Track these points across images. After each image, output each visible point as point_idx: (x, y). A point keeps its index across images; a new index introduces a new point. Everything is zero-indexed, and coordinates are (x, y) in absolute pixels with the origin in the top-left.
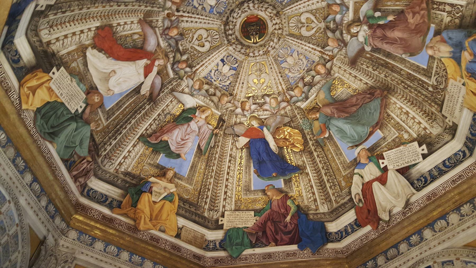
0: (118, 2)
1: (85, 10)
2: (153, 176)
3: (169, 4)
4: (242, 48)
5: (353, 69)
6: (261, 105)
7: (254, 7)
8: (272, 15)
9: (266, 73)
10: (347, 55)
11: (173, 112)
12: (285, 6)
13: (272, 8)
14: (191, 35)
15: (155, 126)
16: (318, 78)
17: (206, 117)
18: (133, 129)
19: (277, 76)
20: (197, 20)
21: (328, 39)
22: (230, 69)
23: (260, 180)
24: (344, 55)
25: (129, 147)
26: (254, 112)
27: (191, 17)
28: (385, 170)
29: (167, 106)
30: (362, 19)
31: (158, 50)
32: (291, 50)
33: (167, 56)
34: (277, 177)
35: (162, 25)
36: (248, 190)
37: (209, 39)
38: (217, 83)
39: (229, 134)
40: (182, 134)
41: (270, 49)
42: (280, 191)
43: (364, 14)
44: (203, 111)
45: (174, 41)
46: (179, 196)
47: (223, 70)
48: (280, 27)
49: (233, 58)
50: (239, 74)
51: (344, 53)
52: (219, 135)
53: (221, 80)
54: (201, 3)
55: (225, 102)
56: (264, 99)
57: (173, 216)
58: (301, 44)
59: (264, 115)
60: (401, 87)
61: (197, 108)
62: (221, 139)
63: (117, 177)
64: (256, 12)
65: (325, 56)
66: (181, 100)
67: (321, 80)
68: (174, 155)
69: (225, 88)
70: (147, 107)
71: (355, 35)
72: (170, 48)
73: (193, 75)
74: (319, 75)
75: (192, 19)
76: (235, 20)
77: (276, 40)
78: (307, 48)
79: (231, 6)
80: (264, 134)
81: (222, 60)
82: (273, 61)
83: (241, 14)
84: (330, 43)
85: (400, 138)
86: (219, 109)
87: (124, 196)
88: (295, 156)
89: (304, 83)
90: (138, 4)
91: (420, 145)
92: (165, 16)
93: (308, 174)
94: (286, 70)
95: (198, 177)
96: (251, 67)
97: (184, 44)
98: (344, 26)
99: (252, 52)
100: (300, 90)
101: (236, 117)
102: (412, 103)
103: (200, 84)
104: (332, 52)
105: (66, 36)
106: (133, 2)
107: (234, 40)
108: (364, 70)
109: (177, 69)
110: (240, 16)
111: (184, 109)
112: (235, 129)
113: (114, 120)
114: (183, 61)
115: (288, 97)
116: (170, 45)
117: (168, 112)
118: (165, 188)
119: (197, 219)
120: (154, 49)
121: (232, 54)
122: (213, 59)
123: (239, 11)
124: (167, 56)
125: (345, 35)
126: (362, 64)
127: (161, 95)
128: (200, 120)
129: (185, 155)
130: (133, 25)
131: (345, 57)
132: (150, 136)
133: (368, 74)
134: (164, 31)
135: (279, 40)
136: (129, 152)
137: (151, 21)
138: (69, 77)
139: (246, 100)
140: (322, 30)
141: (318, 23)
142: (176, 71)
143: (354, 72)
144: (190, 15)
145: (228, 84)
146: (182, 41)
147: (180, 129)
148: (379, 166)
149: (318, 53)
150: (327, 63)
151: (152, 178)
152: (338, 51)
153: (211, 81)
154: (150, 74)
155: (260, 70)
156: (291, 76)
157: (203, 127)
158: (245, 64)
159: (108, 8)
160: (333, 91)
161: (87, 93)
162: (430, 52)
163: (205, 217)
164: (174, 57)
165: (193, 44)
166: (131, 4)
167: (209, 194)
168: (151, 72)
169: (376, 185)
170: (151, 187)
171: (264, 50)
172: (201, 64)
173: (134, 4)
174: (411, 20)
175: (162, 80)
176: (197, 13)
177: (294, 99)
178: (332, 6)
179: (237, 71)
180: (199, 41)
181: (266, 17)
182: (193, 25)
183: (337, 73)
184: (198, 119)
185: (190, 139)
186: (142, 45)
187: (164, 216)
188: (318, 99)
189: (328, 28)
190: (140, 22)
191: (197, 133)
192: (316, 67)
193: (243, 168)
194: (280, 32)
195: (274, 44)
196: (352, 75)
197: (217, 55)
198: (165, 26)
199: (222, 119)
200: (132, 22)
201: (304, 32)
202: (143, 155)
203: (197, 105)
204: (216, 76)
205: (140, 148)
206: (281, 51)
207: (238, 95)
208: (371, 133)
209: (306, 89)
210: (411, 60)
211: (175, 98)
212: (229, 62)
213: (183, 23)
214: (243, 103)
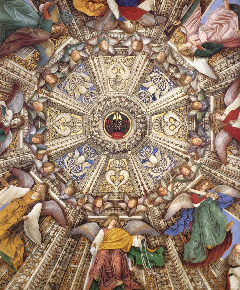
3: (194, 169)
4: (132, 107)
5: (16, 80)
6: (119, 44)
7: (115, 145)
9: (110, 79)
10: (24, 95)
12: (85, 143)
13: (98, 142)
16: (54, 70)
17: (186, 43)
19: (98, 74)
20: (171, 145)
21: (44, 110)
22: (148, 88)
24: (26, 94)
27: (176, 149)
29: (227, 67)
30: (10, 132)
32: (81, 99)
33: (211, 121)
35: (206, 152)
37: (163, 124)
38: (165, 77)
39: (163, 15)
40: (219, 32)
41: (103, 103)
43: (9, 136)
44: (187, 50)
45: (199, 133)
47: (155, 90)
48: (91, 124)
49: (143, 99)
50: (139, 82)
51: (26, 96)
52: (175, 17)
53: (160, 79)
54: (164, 160)
55: (160, 54)
56: (115, 50)
58: (71, 105)
61: (193, 56)
62: (173, 12)
64: (113, 141)
65: (47, 92)
67: (50, 67)
68: (237, 10)
69: (157, 70)
72: (205, 127)
73: (189, 91)
74: (53, 73)
75: (175, 147)
76: (135, 136)
77: (97, 111)
78: (65, 101)
81: (154, 99)
82: (102, 91)
83: (128, 141)
84: (41, 105)
86: (168, 48)
89: (69, 65)
90: (222, 180)
94: (88, 80)
96: (126, 87)
97: (190, 126)
98: (28, 124)
99: (122, 101)
100: (74, 58)
101: (150, 34)
103: (184, 81)
104: (39, 96)
106: (227, 184)
108: (4, 79)
109: (205, 103)
110: (129, 139)
111: (209, 59)
112: (153, 21)
114: (195, 109)
116: (204, 130)
117: (228, 61)
120: (222, 133)
121: (143, 103)
122: (164, 103)
123: (129, 144)
124: (211, 121)
125: (27, 115)
127: (230, 81)
129: (224, 6)
130: (234, 163)
131: (25, 92)
134: (205, 146)
135: (93, 111)
137: (215, 159)
141: (53, 125)
142: (206, 102)
144: (177, 152)
145: (153, 73)
146: (191, 130)
147: (220, 38)
149: (54, 95)
150: (44, 85)
153: (171, 80)
154: (235, 109)
155: (116, 82)
156: (83, 73)
157: (192, 33)
158: (131, 90)
160: (36, 57)
164: (204, 116)
165: (180, 123)
166: (229, 184)
168: (233, 112)
171: (110, 102)
172: (177, 101)
173: (226, 182)
175: (224, 98)
176: (169, 152)
178: (39, 142)
179: (141, 86)
180: (175, 125)
182: (176, 142)
184: (196, 43)
185: (210, 22)
186: (232, 141)
188: (53, 47)
189: (44, 121)
190: (227, 163)
191: (202, 27)
192: (55, 81)
194: (92, 119)
195: (98, 107)
196: (17, 74)
197: (159, 105)
198: (203, 149)
199: (167, 35)
200: (234, 166)
203: (193, 59)
204: (165, 84)
206: (92, 100)
207: (144, 59)
211: (215, 72)
212: (148, 96)
213: (185, 146)
214: (140, 49)
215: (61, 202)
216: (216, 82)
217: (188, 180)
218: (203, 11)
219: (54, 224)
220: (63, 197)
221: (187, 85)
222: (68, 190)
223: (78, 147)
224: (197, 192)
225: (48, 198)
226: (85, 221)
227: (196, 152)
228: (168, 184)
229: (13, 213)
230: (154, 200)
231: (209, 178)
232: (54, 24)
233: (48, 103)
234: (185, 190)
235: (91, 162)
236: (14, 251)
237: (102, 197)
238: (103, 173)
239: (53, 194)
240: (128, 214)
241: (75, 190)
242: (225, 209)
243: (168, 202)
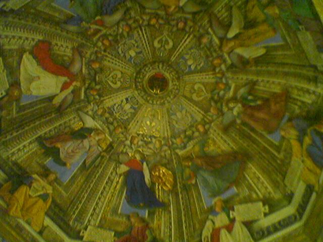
0: (62, 28)
1: (36, 24)
2: (37, 174)
3: (100, 44)
6: (147, 143)
8: (174, 78)
11: (73, 126)
12: (185, 74)
14: (108, 72)
15: (54, 133)
16: (197, 134)
18: (36, 128)
19: (166, 124)
22: (131, 107)
23: (128, 206)
25: (26, 143)
26: (140, 147)
28: (233, 221)
29: (70, 120)
31: (79, 74)
34: (144, 208)
36: (115, 211)
37: (122, 80)
38: (117, 115)
41: (166, 102)
42: (143, 220)
44: (98, 134)
46: (53, 198)
47: (125, 106)
57: (42, 214)
59: (147, 152)
60: (257, 157)
63: (7, 163)
65: (206, 119)
66: (83, 119)
69: (122, 121)
70: (53, 115)
71: (232, 109)
76: (145, 73)
77: (172, 97)
79: (146, 61)
80: (142, 168)
81: (127, 99)
84: (212, 110)
85: (250, 196)
87: (6, 181)
88: (164, 194)
91: (264, 205)
92: (94, 52)
93: (170, 212)
95: (74, 188)
101: (124, 147)
102: (264, 170)
105: (14, 37)
107: (140, 86)
109: (89, 94)
112: (120, 157)
113: (23, 116)
115: (170, 142)
116: (89, 74)
118: (43, 187)
119: (62, 224)
121: (137, 98)
124: (84, 81)
125: (224, 107)
126: (232, 133)
127: (69, 109)
128: (93, 140)
129: (70, 165)
131: (221, 124)
132: (46, 139)
133: (234, 141)
135: (174, 98)
136: (24, 146)
138: (3, 68)
139: (136, 135)
140: (208, 98)
143: (224, 137)
148: (228, 216)
151: (36, 175)
152: (216, 119)
154: (65, 91)
155: (154, 116)
159: (53, 30)
161: (11, 85)
162: (283, 133)
163: (69, 225)
164: (89, 84)
165: (108, 79)
167: (80, 206)
168: (68, 88)
169: (223, 232)
170: (32, 183)
172: (109, 96)
174: (273, 107)
177: (175, 145)
179: (136, 111)
181: (169, 78)
183: (212, 135)
187: (35, 211)
189: (212, 98)
190: (73, 49)
193: (117, 193)
194: (177, 91)
198: (92, 58)
201: (195, 97)
202: (35, 153)
205: (35, 147)
208: (228, 188)
209: (185, 140)
210: (269, 137)
211: (79, 116)
215: (212, 33)
216: (79, 109)
217: (105, 37)
218: (85, 162)
219: (220, 17)
220: (210, 36)
221: (101, 108)
222: (205, 40)
223: (191, 72)
224: (97, 27)
225: (221, 40)
226: (194, 14)
227: (97, 57)
228: (122, 33)
229: (249, 38)
230: (134, 22)
231: (88, 38)
232: (189, 167)
233: (207, 111)
234: (107, 29)
235: (184, 58)
236: (254, 10)
237: (178, 30)
238: (175, 47)
239: (216, 41)
240: (157, 14)
241: (199, 38)
242: (74, 16)
243: (123, 19)
